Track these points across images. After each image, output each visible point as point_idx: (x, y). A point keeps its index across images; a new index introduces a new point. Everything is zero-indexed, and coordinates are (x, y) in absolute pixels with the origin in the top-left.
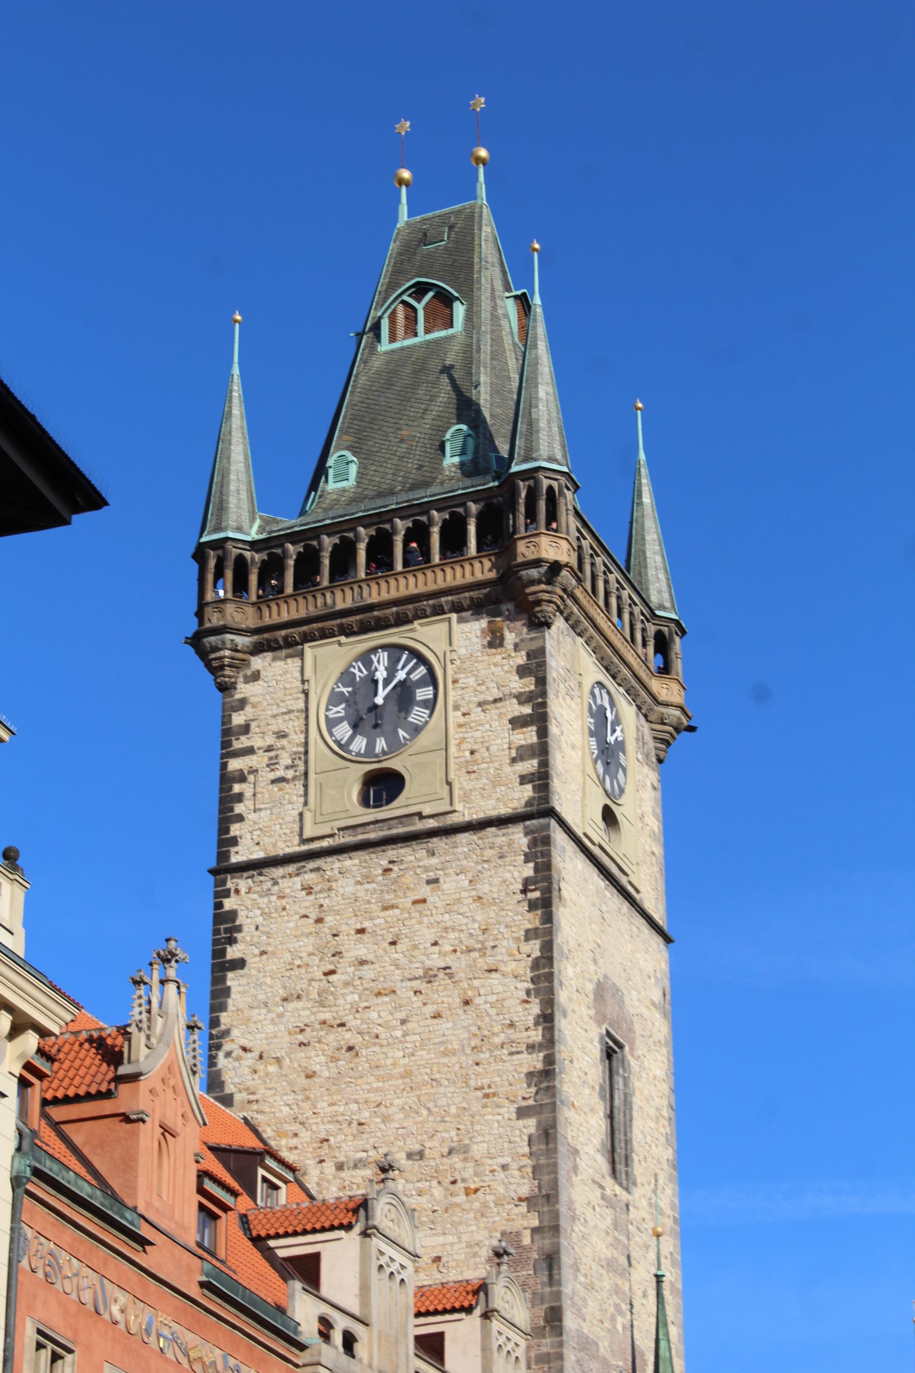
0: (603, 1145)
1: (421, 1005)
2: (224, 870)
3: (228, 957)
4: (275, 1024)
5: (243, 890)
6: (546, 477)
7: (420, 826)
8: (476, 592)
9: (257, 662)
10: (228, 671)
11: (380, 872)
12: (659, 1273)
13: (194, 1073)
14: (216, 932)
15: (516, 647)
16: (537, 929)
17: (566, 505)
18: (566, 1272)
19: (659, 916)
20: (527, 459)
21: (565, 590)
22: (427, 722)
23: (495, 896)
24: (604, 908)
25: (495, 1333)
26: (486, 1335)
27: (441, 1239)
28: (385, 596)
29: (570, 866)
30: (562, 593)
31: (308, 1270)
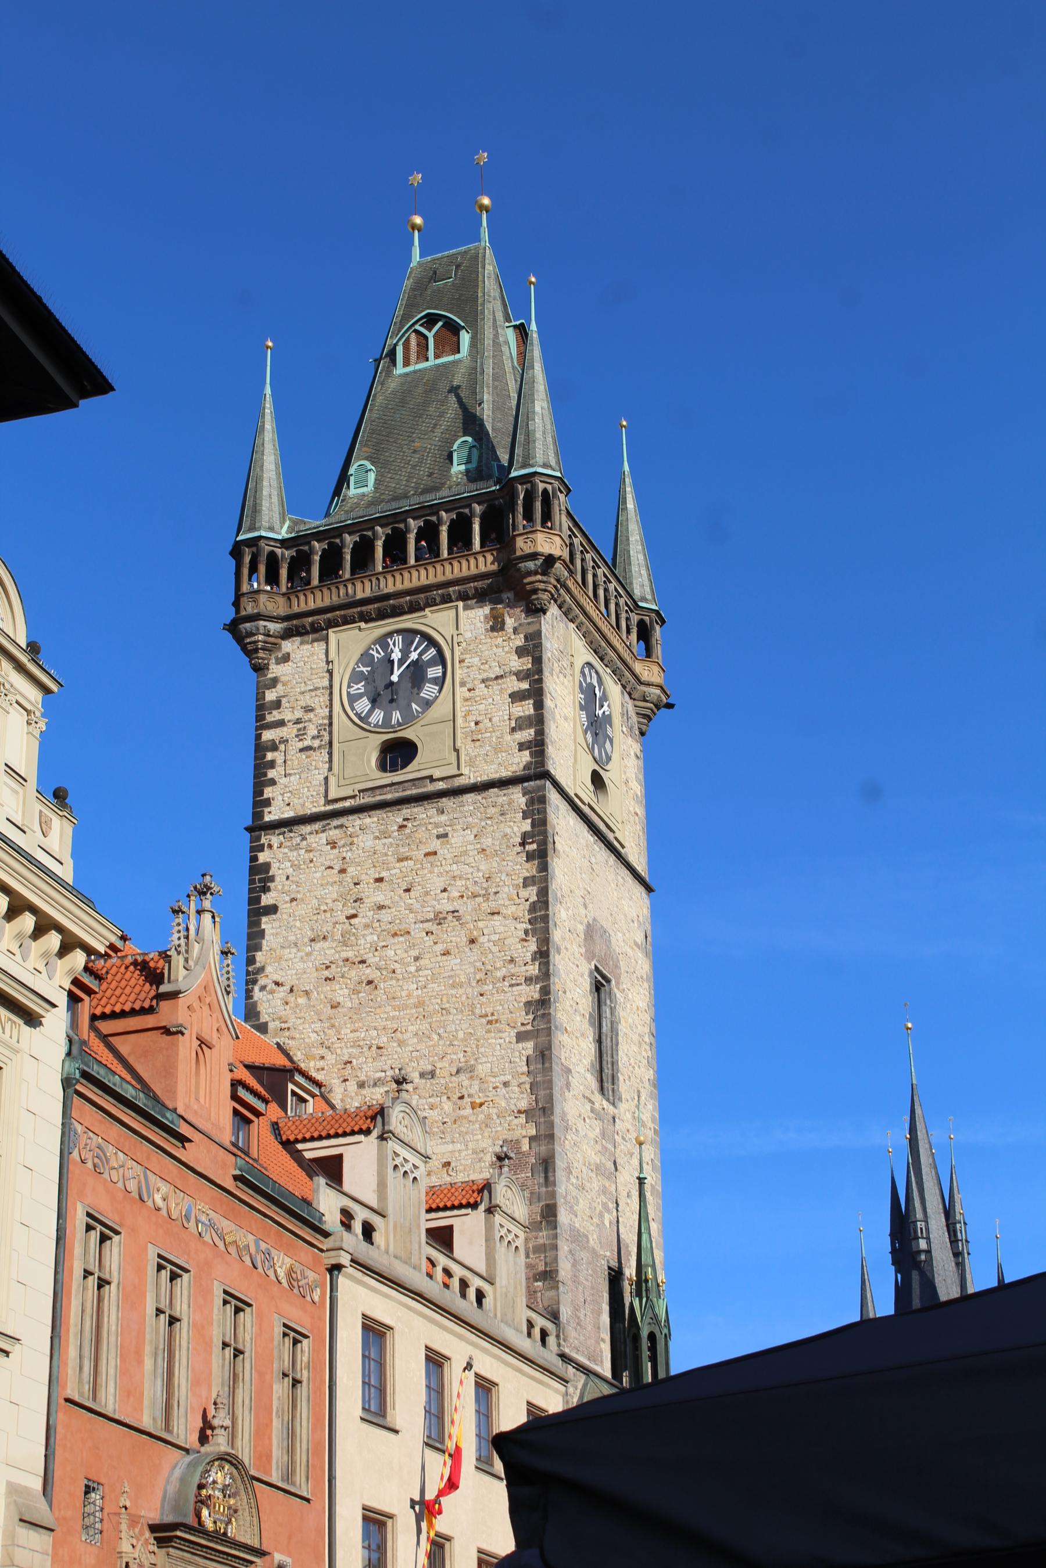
0: (592, 1065)
2: (258, 827)
3: (263, 904)
5: (275, 846)
7: (431, 788)
9: (287, 646)
10: (261, 654)
12: (642, 1176)
13: (228, 993)
14: (252, 882)
15: (515, 631)
16: (534, 877)
18: (560, 1175)
19: (641, 868)
20: (524, 466)
21: (558, 581)
24: (593, 860)
25: (497, 1226)
26: (489, 1228)
27: (450, 1147)
28: (399, 586)
29: (563, 823)
30: (555, 583)
31: (331, 1169)
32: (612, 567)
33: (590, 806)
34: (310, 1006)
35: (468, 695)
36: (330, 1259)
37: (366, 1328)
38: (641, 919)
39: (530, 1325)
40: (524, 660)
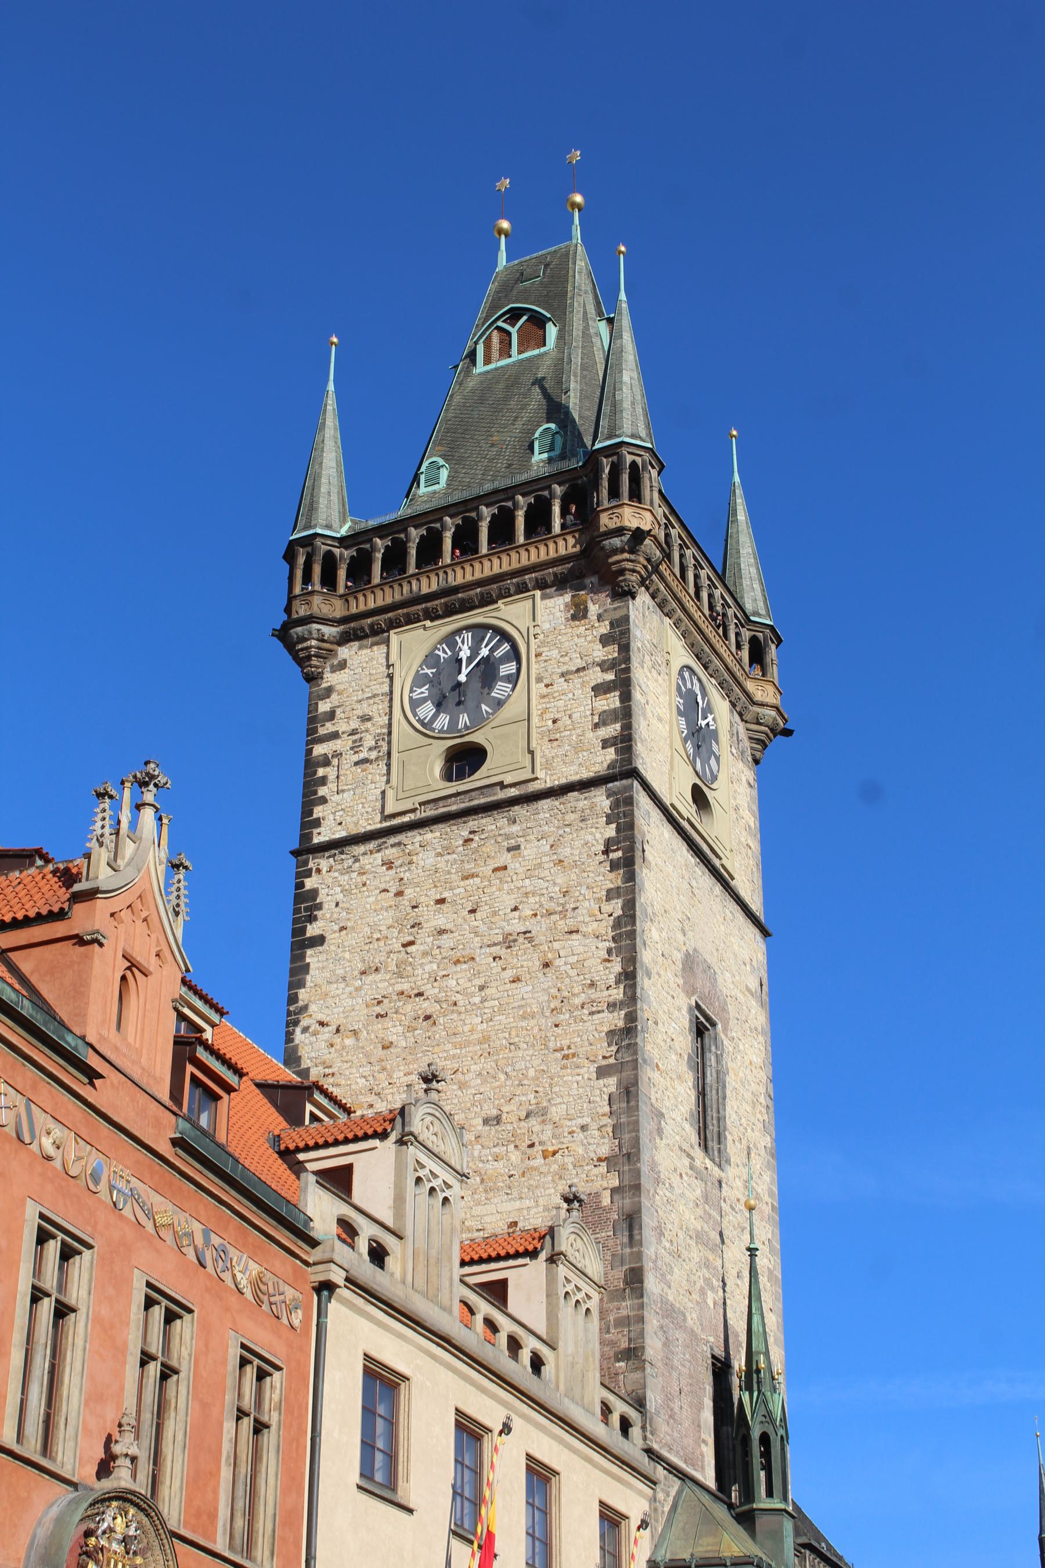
0: (692, 1115)
2: (306, 850)
3: (308, 935)
4: (353, 998)
6: (629, 453)
7: (501, 795)
8: (560, 568)
9: (344, 652)
10: (314, 661)
11: (461, 842)
12: (752, 1246)
13: (177, 914)
14: (297, 911)
15: (600, 618)
17: (651, 482)
18: (648, 1233)
20: (609, 438)
21: (649, 560)
24: (694, 884)
25: (561, 1279)
26: (551, 1280)
27: (517, 1204)
28: (469, 578)
29: (655, 834)
30: (645, 563)
31: (339, 1180)
32: (722, 578)
33: (689, 821)
34: (359, 1048)
35: (545, 691)
36: (318, 1275)
37: (368, 1372)
38: (755, 963)
39: (606, 1410)
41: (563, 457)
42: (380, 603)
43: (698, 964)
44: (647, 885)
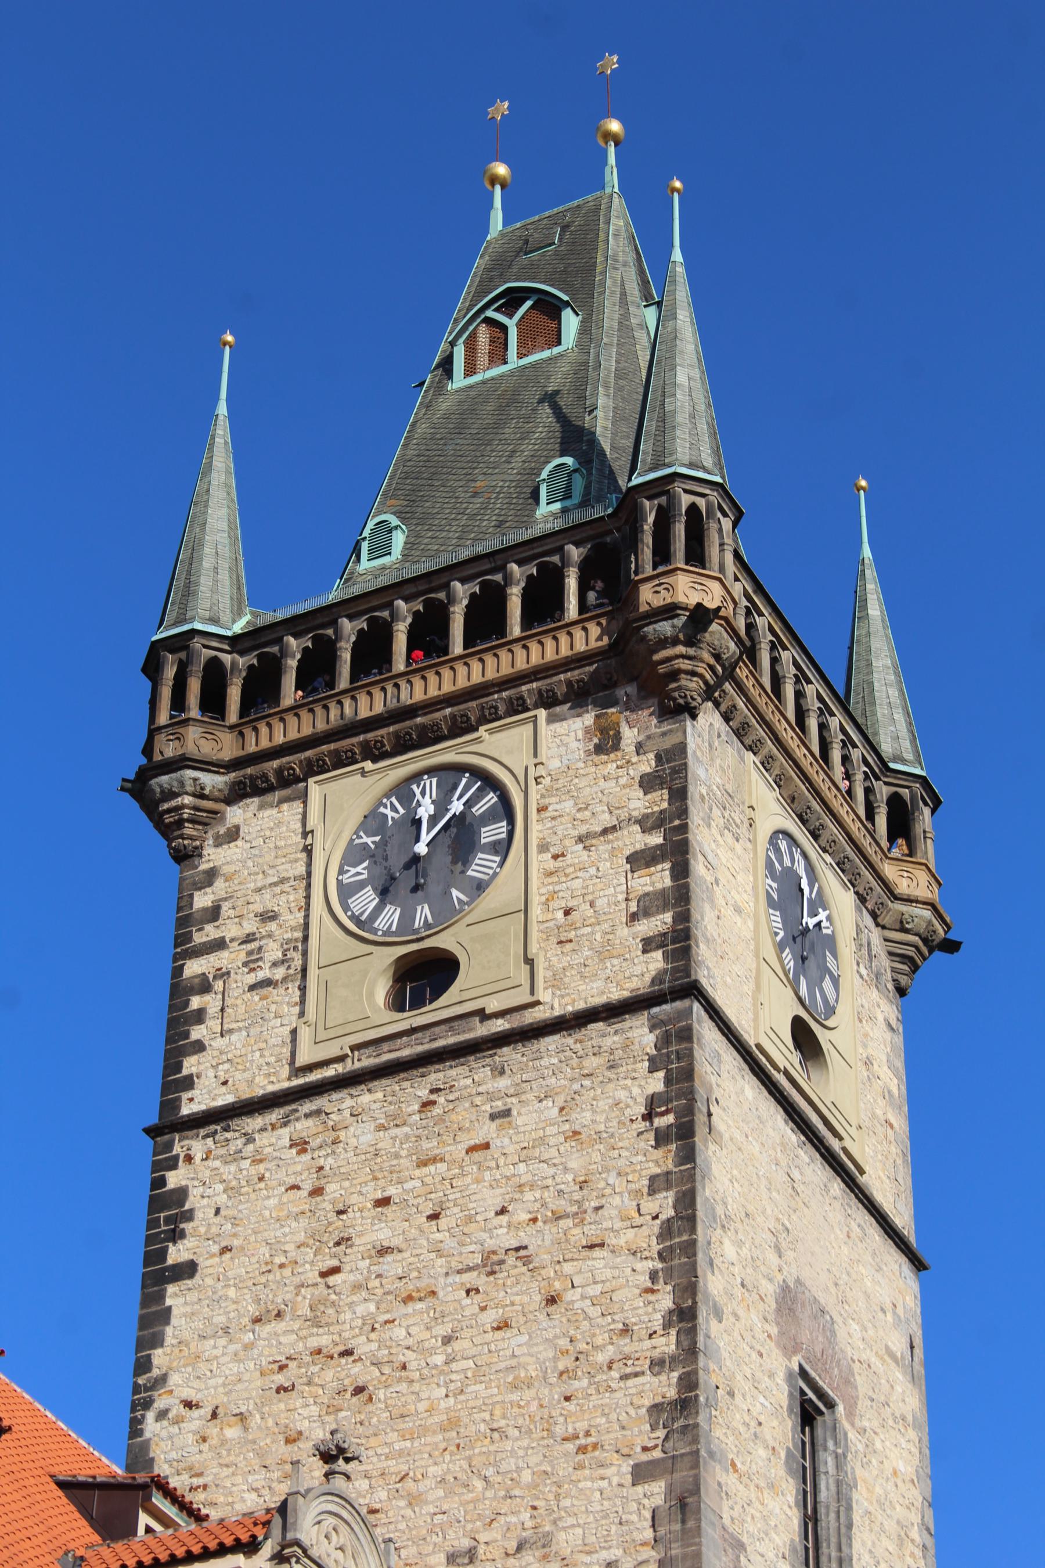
0: (793, 1550)
1: (477, 1310)
2: (169, 1126)
3: (170, 1261)
4: (240, 1361)
6: (686, 491)
7: (481, 1030)
8: (576, 672)
9: (235, 814)
10: (189, 830)
11: (416, 1107)
14: (152, 1223)
15: (639, 748)
16: (668, 1173)
17: (721, 537)
21: (717, 657)
22: (495, 874)
23: (602, 1128)
24: (796, 1174)
28: (433, 692)
30: (712, 661)
33: (786, 1073)
34: (248, 1442)
35: (552, 865)
38: (900, 1311)
40: (656, 795)
41: (585, 503)
42: (293, 735)
43: (803, 1305)
44: (716, 1169)
